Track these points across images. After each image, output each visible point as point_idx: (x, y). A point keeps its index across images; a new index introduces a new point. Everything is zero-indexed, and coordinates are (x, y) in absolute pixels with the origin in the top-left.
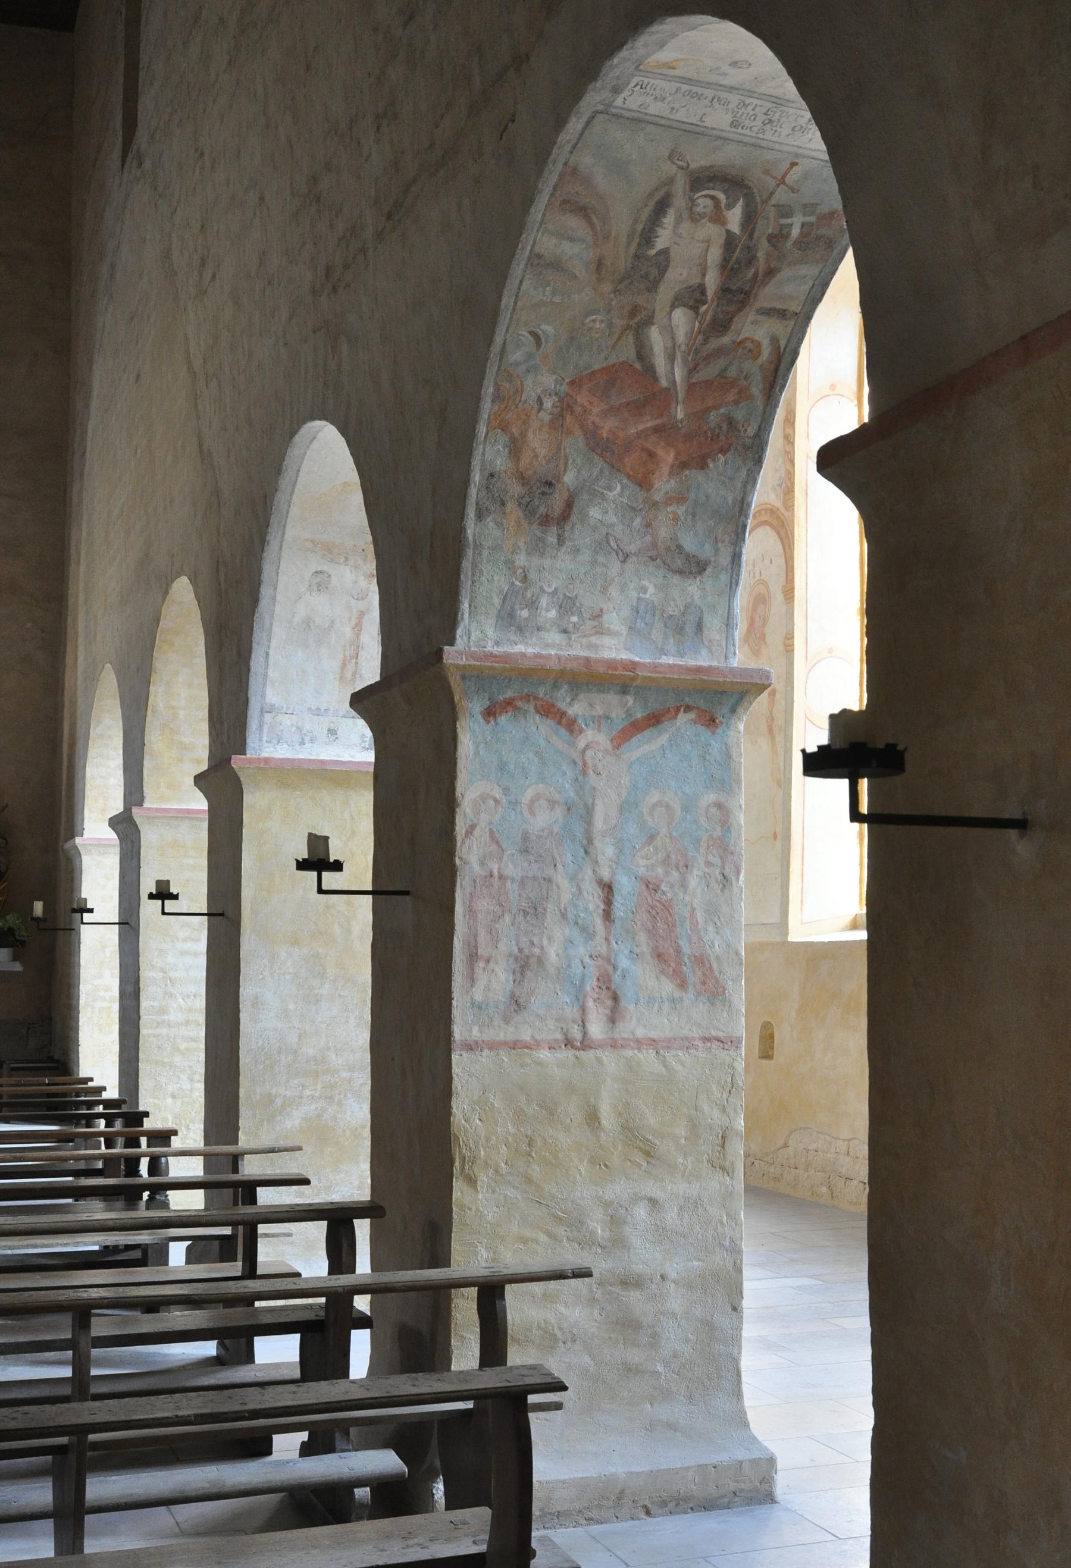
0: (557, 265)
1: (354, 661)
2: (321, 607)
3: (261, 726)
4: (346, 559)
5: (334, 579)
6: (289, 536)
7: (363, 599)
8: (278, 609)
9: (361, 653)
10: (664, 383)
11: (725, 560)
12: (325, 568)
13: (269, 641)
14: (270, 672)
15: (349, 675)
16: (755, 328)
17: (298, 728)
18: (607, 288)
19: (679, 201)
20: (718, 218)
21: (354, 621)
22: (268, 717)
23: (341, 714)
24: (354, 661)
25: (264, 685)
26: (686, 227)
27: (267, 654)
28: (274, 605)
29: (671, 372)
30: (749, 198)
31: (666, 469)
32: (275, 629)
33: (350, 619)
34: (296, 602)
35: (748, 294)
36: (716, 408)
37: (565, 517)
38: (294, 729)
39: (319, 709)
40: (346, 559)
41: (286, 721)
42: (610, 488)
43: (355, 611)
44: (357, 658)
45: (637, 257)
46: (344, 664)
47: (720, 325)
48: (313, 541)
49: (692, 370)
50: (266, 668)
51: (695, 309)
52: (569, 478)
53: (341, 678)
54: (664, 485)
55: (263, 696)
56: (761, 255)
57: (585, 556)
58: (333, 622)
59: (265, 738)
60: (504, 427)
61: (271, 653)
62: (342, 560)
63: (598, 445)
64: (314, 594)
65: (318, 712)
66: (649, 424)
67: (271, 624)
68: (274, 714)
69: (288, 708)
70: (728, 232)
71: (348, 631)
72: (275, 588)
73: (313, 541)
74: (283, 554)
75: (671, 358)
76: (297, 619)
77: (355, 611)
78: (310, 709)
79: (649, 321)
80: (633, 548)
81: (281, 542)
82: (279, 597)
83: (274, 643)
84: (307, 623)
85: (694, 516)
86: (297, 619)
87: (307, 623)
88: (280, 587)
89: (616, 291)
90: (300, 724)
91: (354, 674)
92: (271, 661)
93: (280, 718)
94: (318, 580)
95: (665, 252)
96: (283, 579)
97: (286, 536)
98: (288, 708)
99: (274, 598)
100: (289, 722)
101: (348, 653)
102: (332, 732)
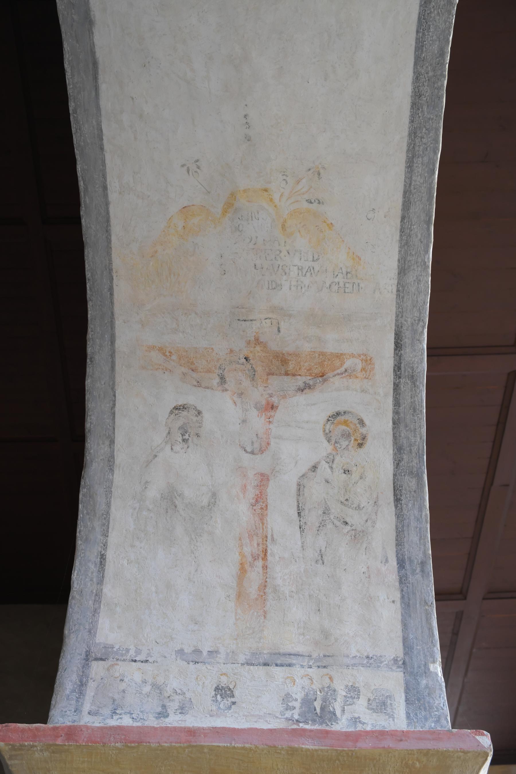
1: (260, 563)
2: (191, 469)
3: (82, 685)
4: (223, 379)
5: (207, 416)
6: (122, 344)
7: (262, 451)
8: (118, 478)
9: (272, 548)
12: (191, 397)
13: (106, 535)
14: (108, 590)
15: (253, 590)
17: (155, 686)
21: (252, 492)
22: (97, 669)
23: (242, 658)
24: (260, 563)
25: (96, 612)
27: (103, 557)
28: (112, 470)
32: (116, 513)
33: (244, 488)
34: (148, 463)
38: (147, 689)
39: (197, 651)
40: (223, 379)
41: (134, 674)
43: (251, 474)
44: (265, 558)
46: (243, 570)
48: (161, 350)
50: (101, 582)
53: (241, 595)
55: (92, 632)
58: (214, 495)
59: (87, 707)
61: (110, 555)
62: (216, 381)
64: (177, 448)
65: (195, 657)
67: (108, 505)
68: (109, 662)
69: (138, 652)
71: (243, 511)
72: (112, 442)
73: (161, 350)
74: (118, 379)
76: (152, 493)
77: (251, 474)
78: (180, 652)
81: (112, 355)
82: (120, 458)
83: (113, 538)
84: (171, 499)
86: (152, 493)
87: (171, 499)
88: (120, 438)
90: (160, 680)
91: (264, 586)
92: (110, 569)
93: (122, 668)
94: (180, 423)
96: (122, 424)
97: (118, 343)
98: (138, 652)
99: (111, 460)
100: (138, 677)
101: (247, 550)
102: (224, 692)
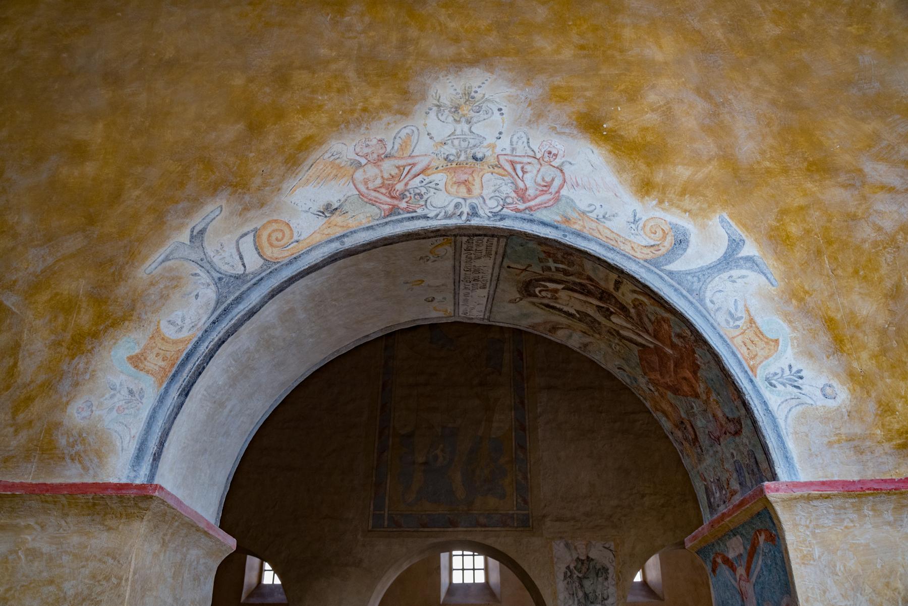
0: (586, 345)
10: (652, 346)
11: (743, 411)
16: (626, 296)
18: (597, 336)
19: (546, 301)
20: (556, 291)
26: (560, 301)
29: (647, 339)
30: (537, 280)
31: (694, 381)
35: (603, 292)
36: (670, 337)
37: (696, 435)
42: (692, 408)
45: (580, 320)
47: (623, 309)
49: (647, 332)
51: (612, 313)
52: (683, 415)
54: (701, 388)
56: (578, 280)
57: (711, 452)
60: (657, 410)
63: (676, 391)
66: (672, 366)
70: (563, 289)
75: (639, 335)
79: (618, 333)
80: (718, 433)
85: (719, 394)
89: (599, 334)
95: (578, 312)
